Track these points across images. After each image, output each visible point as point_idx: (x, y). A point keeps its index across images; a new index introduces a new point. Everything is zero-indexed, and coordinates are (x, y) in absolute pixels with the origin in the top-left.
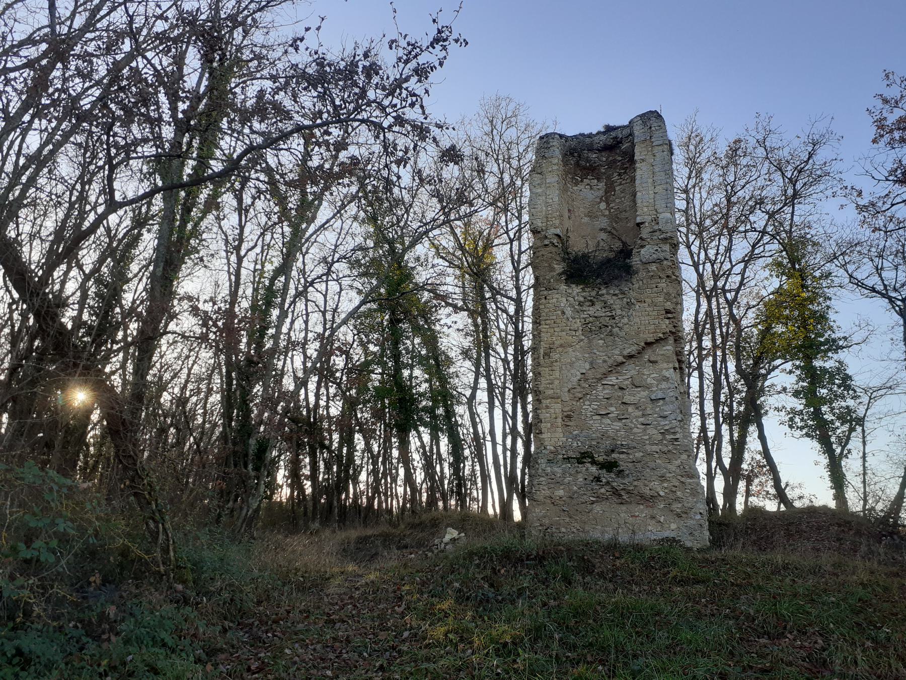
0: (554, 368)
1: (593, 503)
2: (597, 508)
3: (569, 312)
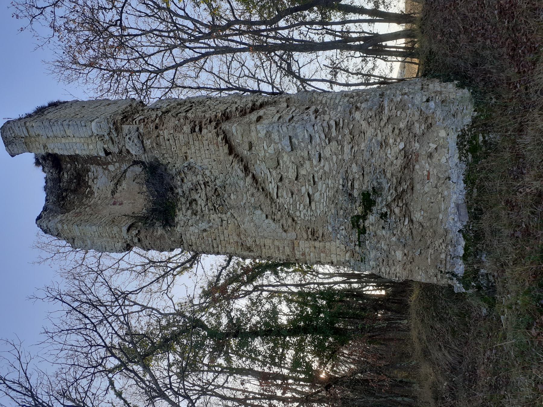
0: (262, 244)
1: (411, 221)
2: (417, 216)
3: (204, 225)
